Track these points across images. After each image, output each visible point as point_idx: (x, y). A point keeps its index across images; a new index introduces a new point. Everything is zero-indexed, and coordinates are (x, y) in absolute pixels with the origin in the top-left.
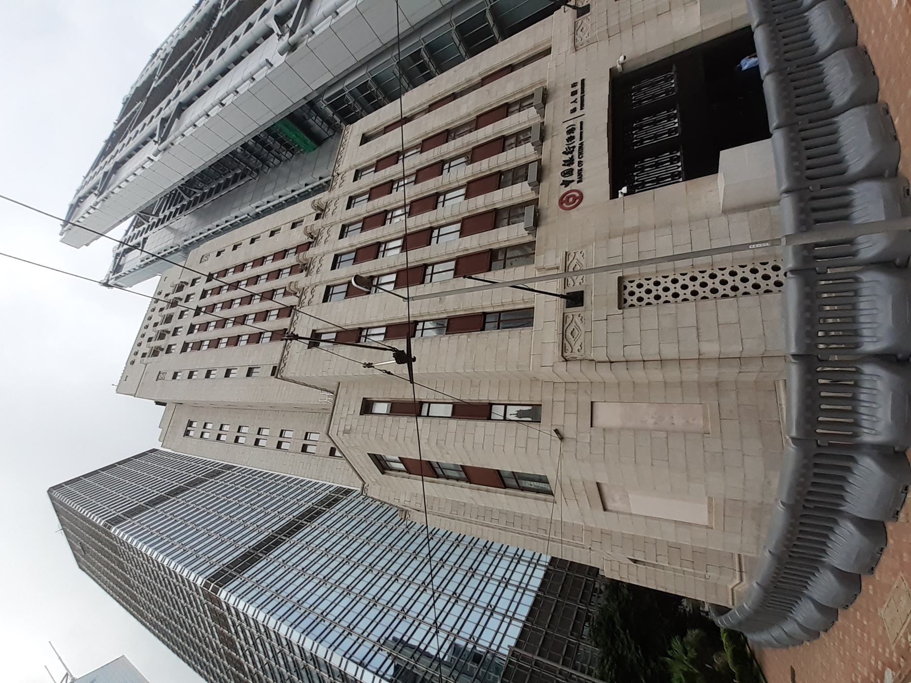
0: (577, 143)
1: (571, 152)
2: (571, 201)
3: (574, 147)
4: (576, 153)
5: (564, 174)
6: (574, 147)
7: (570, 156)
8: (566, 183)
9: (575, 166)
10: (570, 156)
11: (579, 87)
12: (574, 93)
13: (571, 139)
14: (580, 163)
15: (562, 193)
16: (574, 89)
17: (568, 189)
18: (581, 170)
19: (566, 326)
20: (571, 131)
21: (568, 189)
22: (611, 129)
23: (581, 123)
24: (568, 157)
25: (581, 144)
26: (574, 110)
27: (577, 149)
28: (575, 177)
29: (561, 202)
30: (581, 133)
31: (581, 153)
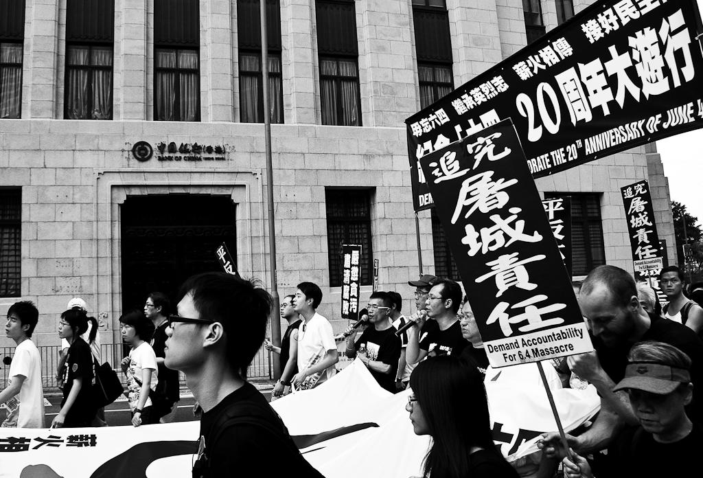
0: (204, 155)
1: (193, 151)
5: (173, 144)
8: (162, 148)
9: (178, 154)
13: (209, 150)
17: (154, 147)
20: (219, 150)
23: (223, 159)
28: (166, 154)
30: (212, 159)
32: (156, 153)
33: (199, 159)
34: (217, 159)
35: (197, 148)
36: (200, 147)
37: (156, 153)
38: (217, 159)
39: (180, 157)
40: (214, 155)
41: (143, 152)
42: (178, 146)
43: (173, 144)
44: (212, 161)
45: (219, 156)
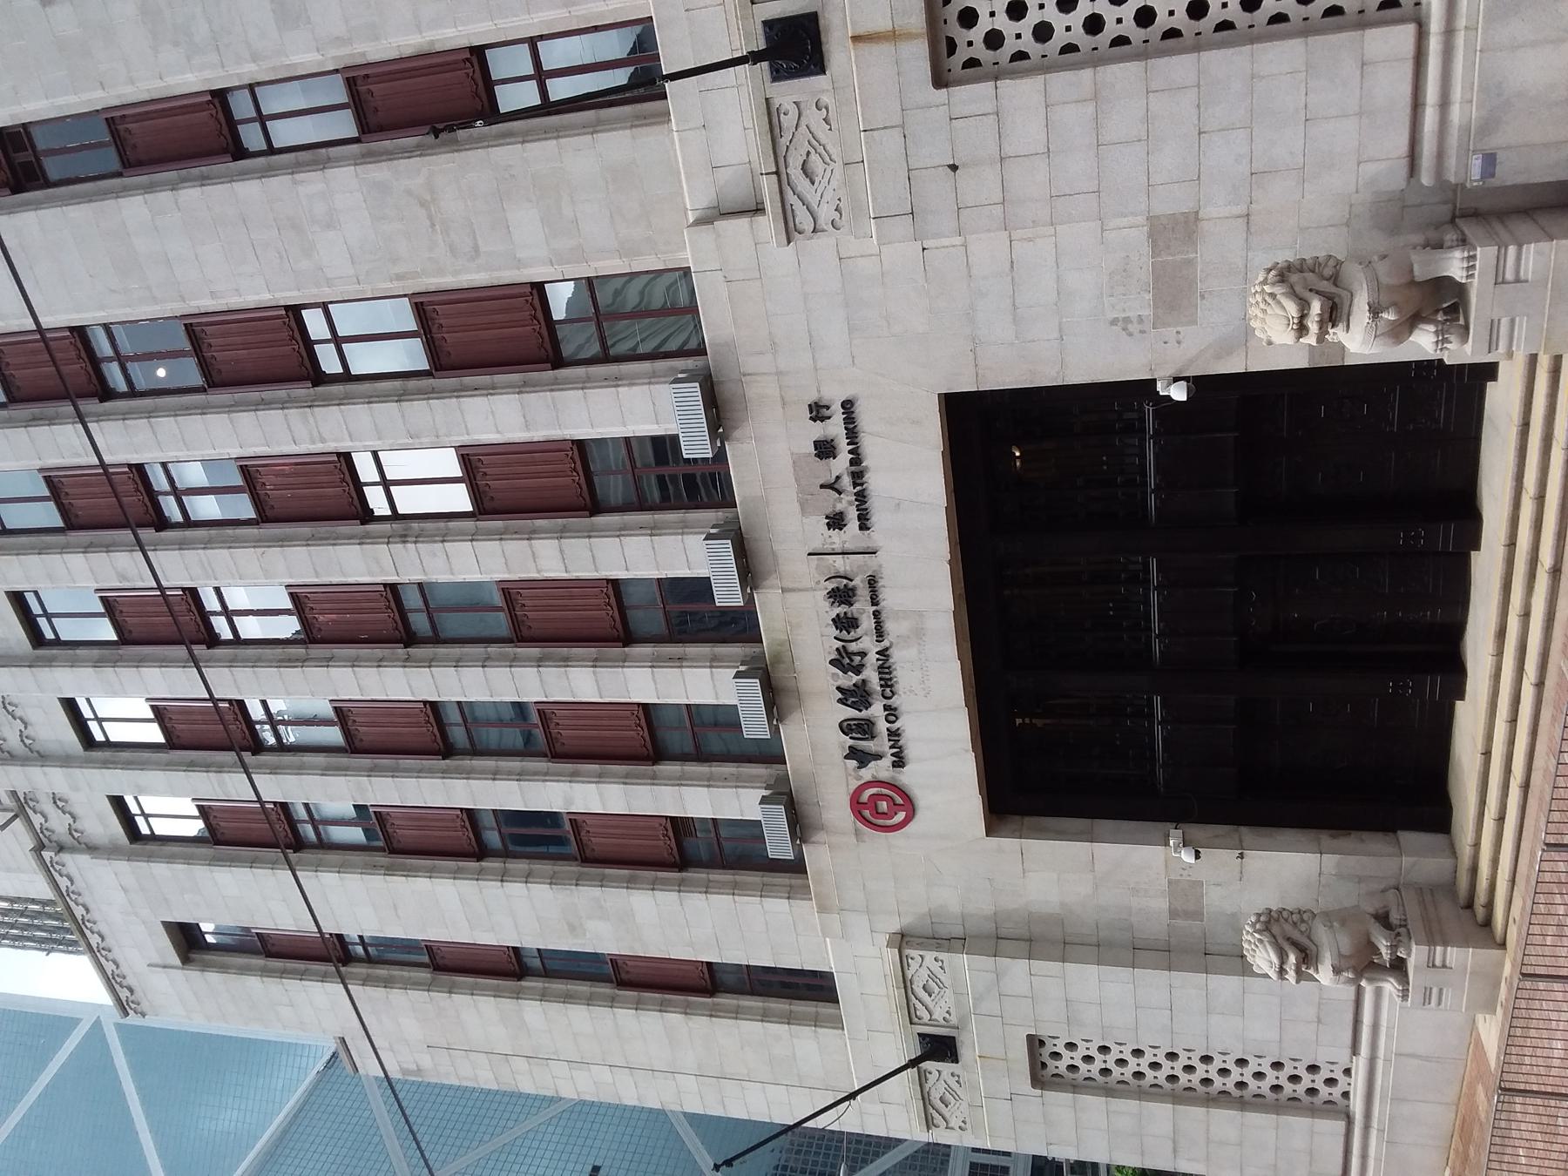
1: (858, 670)
2: (884, 808)
3: (863, 654)
4: (871, 675)
5: (846, 728)
6: (863, 654)
7: (855, 679)
8: (861, 757)
9: (876, 710)
10: (855, 679)
11: (835, 428)
12: (825, 449)
13: (846, 624)
14: (892, 713)
15: (854, 784)
16: (818, 431)
17: (867, 774)
18: (894, 735)
19: (784, 141)
20: (842, 595)
21: (867, 774)
22: (974, 701)
23: (872, 582)
24: (851, 680)
25: (884, 653)
26: (836, 521)
27: (872, 659)
28: (881, 744)
29: (857, 805)
30: (876, 614)
31: (887, 683)
32: (881, 769)
33: (884, 653)
34: (874, 601)
35: (845, 660)
36: (843, 652)
37: (881, 769)
38: (874, 601)
39: (886, 708)
40: (862, 607)
41: (883, 806)
42: (852, 713)
43: (846, 728)
44: (884, 616)
45: (863, 593)
